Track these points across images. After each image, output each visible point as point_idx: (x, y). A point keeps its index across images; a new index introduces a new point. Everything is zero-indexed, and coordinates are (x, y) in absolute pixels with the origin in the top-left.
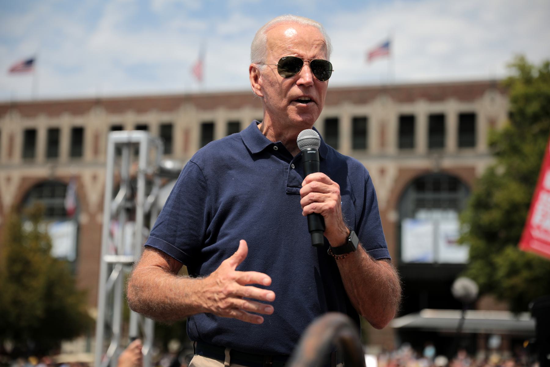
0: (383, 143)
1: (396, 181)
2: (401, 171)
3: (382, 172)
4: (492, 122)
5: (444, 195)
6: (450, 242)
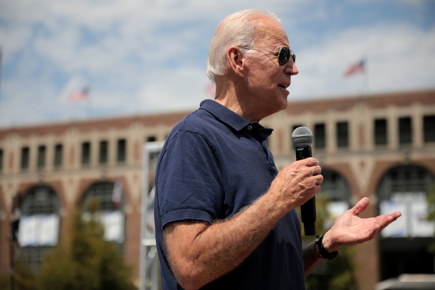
2: (378, 164)
3: (362, 165)
5: (414, 181)
6: (421, 220)
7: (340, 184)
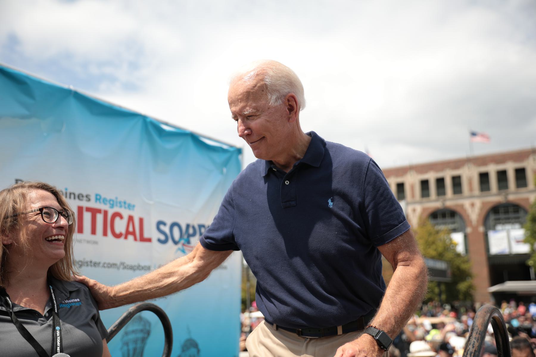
0: (471, 189)
1: (481, 209)
2: (484, 204)
3: (473, 205)
5: (511, 215)
6: (518, 242)
7: (457, 219)
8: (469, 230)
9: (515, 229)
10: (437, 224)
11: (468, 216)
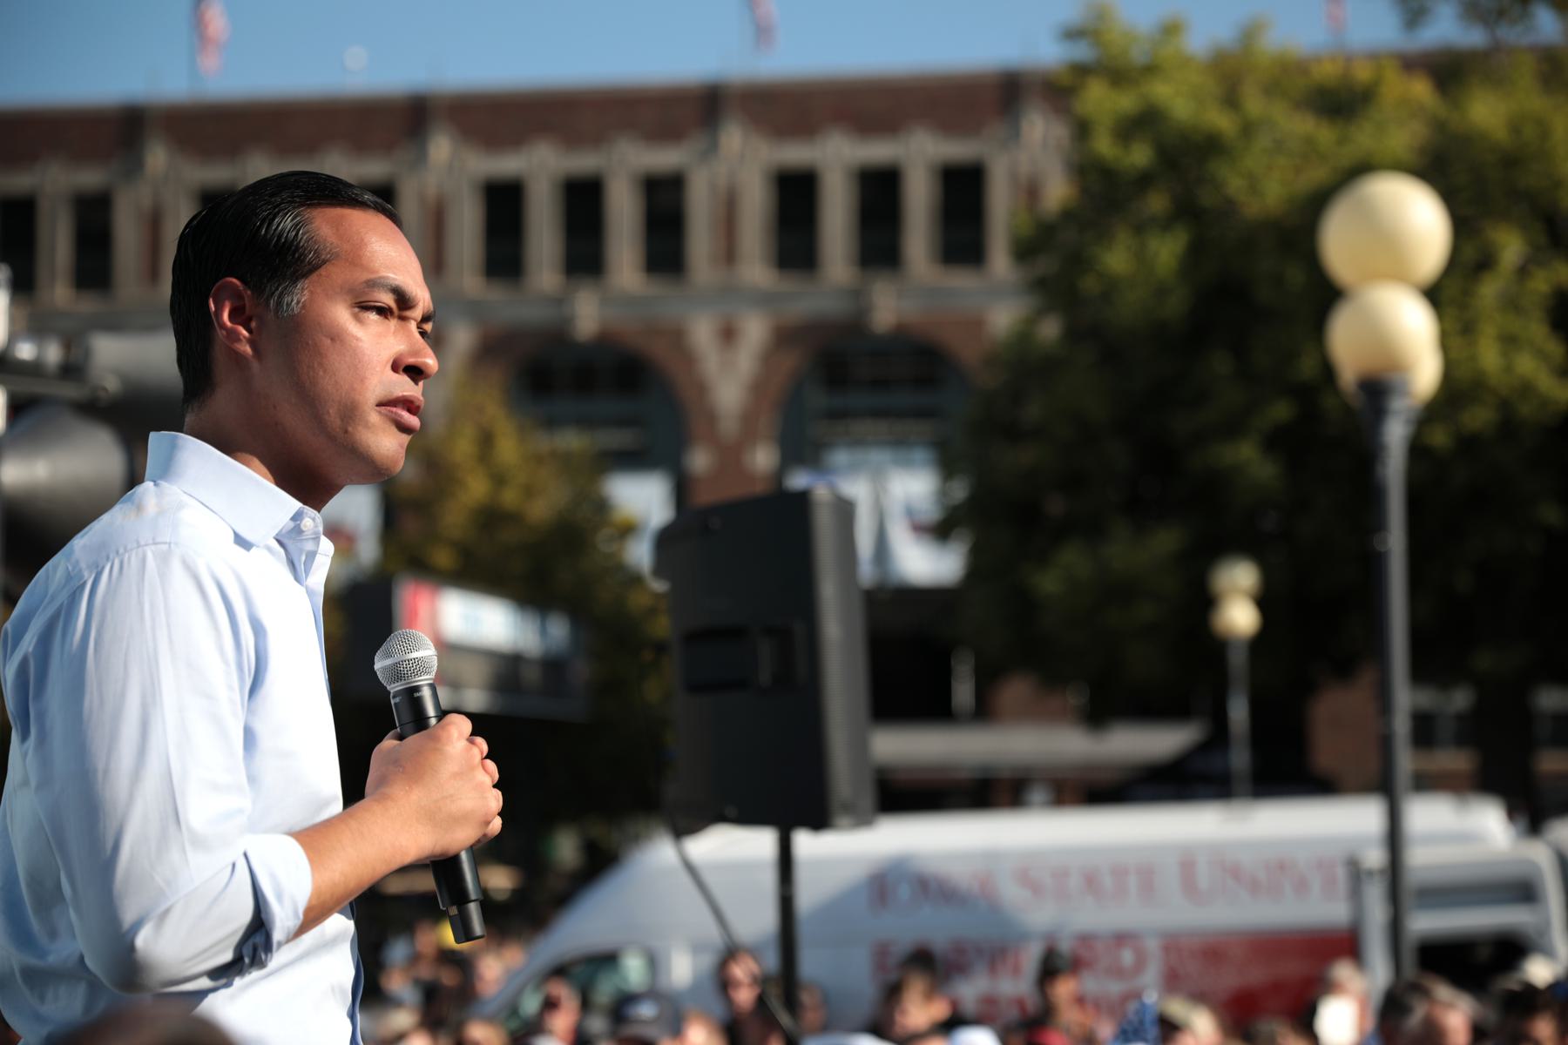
3: (728, 334)
4: (1032, 192)
8: (700, 460)
9: (907, 464)
10: (551, 423)
11: (702, 389)
